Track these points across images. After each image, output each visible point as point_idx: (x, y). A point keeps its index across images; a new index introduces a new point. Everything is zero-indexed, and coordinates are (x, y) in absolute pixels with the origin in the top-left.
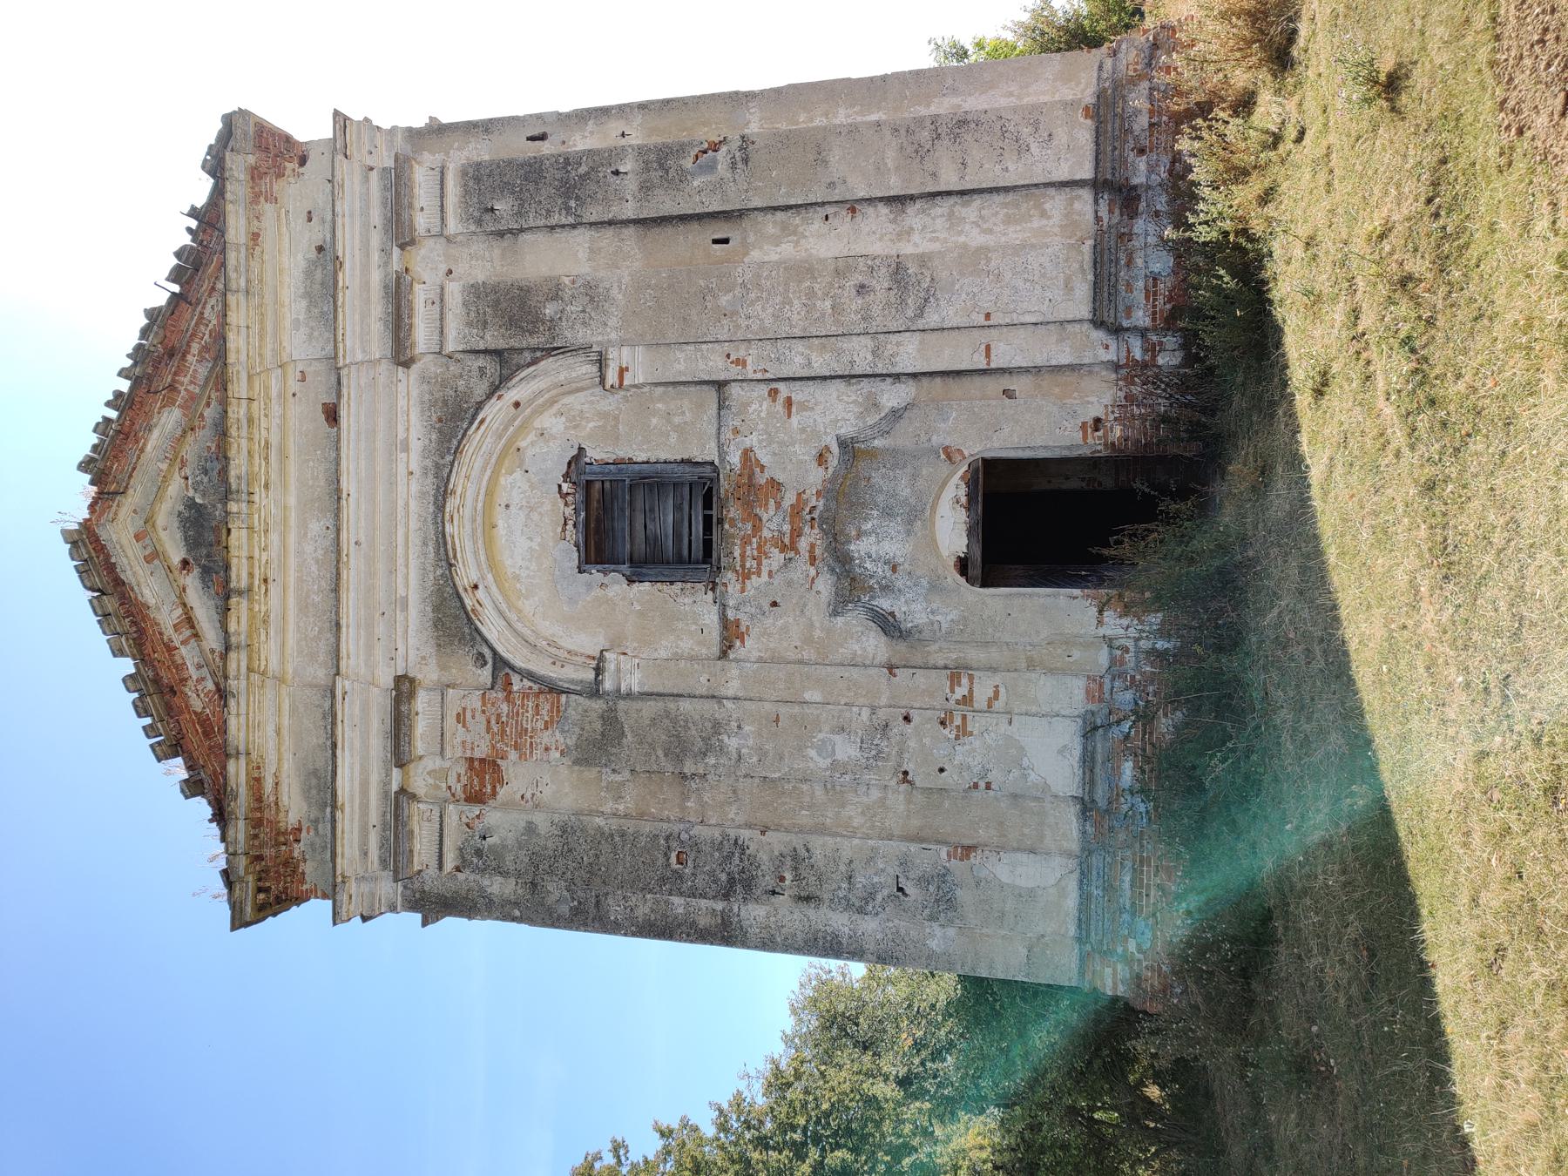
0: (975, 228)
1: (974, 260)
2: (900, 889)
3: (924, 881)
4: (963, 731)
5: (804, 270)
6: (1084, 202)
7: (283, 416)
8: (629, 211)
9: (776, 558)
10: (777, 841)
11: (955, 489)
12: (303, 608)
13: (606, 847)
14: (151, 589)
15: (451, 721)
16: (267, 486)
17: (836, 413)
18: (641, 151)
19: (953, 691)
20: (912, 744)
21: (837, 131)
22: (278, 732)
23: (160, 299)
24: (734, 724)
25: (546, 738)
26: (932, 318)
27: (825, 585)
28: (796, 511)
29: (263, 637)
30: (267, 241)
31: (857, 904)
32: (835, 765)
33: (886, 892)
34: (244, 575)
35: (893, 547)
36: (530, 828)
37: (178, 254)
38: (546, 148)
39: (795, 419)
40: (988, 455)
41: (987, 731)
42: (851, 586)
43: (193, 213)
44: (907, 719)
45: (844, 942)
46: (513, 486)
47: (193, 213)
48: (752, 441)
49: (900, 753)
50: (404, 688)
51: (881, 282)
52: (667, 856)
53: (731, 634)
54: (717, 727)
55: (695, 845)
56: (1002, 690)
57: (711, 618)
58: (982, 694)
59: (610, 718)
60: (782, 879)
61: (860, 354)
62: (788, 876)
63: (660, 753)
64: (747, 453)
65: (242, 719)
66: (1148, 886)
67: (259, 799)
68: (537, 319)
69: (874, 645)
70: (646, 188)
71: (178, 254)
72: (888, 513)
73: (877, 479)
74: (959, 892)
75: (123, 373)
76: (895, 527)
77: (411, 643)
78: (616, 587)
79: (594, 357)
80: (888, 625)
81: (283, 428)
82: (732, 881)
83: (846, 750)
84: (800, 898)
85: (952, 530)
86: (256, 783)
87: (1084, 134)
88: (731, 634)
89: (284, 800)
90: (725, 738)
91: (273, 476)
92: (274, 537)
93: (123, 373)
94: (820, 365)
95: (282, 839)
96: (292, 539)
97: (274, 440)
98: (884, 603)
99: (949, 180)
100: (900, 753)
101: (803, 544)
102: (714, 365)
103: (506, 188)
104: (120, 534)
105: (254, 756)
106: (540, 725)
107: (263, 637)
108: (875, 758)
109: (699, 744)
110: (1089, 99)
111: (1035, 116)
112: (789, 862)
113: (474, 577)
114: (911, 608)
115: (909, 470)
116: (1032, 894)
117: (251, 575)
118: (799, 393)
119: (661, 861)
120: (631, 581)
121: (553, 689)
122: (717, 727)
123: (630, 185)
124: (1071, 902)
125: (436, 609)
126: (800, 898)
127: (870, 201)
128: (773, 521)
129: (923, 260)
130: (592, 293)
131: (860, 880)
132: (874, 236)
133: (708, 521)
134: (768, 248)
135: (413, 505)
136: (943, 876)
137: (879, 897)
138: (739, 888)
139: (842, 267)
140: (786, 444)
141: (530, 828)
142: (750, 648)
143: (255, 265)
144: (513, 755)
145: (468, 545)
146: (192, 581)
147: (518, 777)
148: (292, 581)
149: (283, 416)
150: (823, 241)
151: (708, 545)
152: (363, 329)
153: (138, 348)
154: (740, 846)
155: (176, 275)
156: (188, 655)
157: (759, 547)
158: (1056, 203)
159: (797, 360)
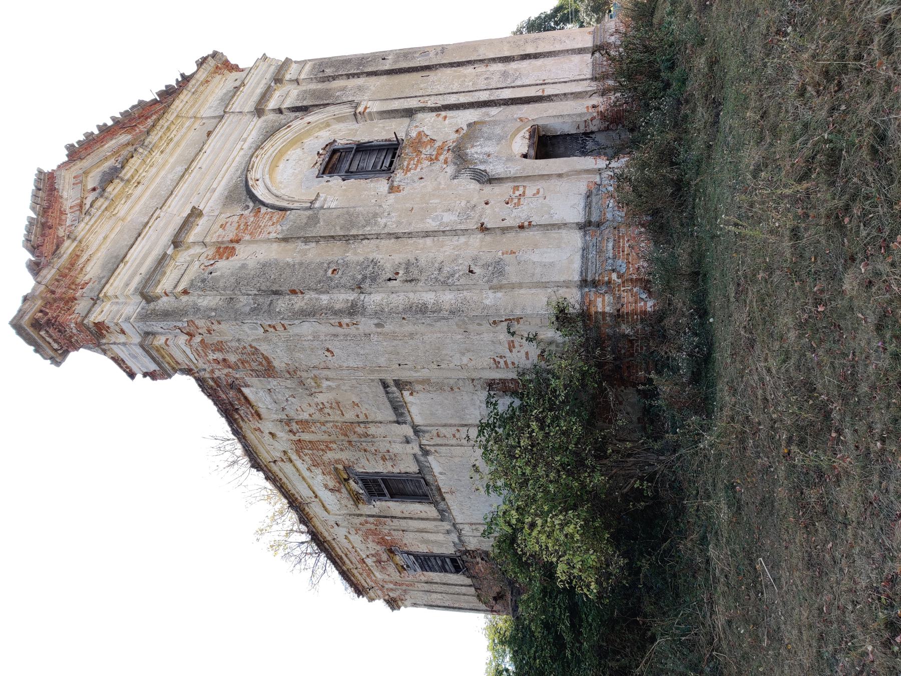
2: (471, 271)
3: (486, 266)
4: (518, 204)
6: (588, 57)
7: (186, 133)
8: (387, 68)
9: (427, 163)
10: (398, 258)
11: (525, 132)
12: (152, 197)
13: (288, 270)
15: (217, 226)
16: (162, 152)
19: (514, 193)
20: (488, 212)
22: (105, 238)
23: (149, 97)
24: (386, 214)
25: (271, 229)
26: (519, 83)
27: (450, 169)
28: (441, 148)
29: (122, 202)
30: (212, 85)
31: (442, 280)
32: (440, 225)
33: (461, 273)
34: (129, 175)
37: (166, 86)
39: (447, 121)
40: (540, 123)
43: (182, 75)
44: (487, 203)
45: (430, 307)
47: (182, 75)
48: (425, 129)
49: (481, 216)
52: (326, 271)
54: (375, 215)
55: (346, 265)
56: (541, 190)
58: (530, 192)
60: (397, 273)
61: (484, 96)
62: (401, 272)
63: (338, 228)
64: (419, 133)
65: (88, 227)
66: (623, 247)
67: (73, 265)
69: (474, 186)
70: (395, 62)
71: (166, 86)
72: (489, 139)
73: (485, 129)
74: (507, 268)
75: (113, 118)
76: (489, 143)
77: (210, 204)
78: (335, 181)
79: (354, 105)
81: (183, 137)
82: (365, 278)
83: (449, 218)
84: (407, 281)
85: (521, 144)
86: (75, 257)
88: (392, 189)
89: (88, 268)
90: (379, 219)
91: (168, 150)
92: (154, 170)
93: (113, 118)
94: (463, 99)
95: (73, 287)
96: (162, 173)
97: (175, 140)
98: (482, 167)
99: (530, 50)
100: (481, 216)
101: (442, 158)
102: (413, 104)
105: (83, 244)
106: (271, 223)
107: (122, 202)
108: (466, 219)
109: (363, 222)
112: (403, 266)
113: (258, 177)
114: (495, 168)
115: (501, 125)
116: (552, 264)
117: (132, 177)
118: (450, 113)
119: (322, 272)
120: (344, 180)
122: (375, 215)
124: (577, 264)
125: (230, 192)
126: (407, 281)
127: (494, 60)
128: (427, 151)
129: (516, 70)
131: (446, 269)
135: (238, 159)
136: (498, 263)
137: (457, 275)
138: (368, 280)
143: (202, 88)
144: (247, 237)
145: (261, 167)
148: (152, 187)
149: (186, 133)
153: (127, 111)
154: (374, 262)
155: (160, 94)
157: (418, 161)
158: (576, 58)
159: (452, 100)
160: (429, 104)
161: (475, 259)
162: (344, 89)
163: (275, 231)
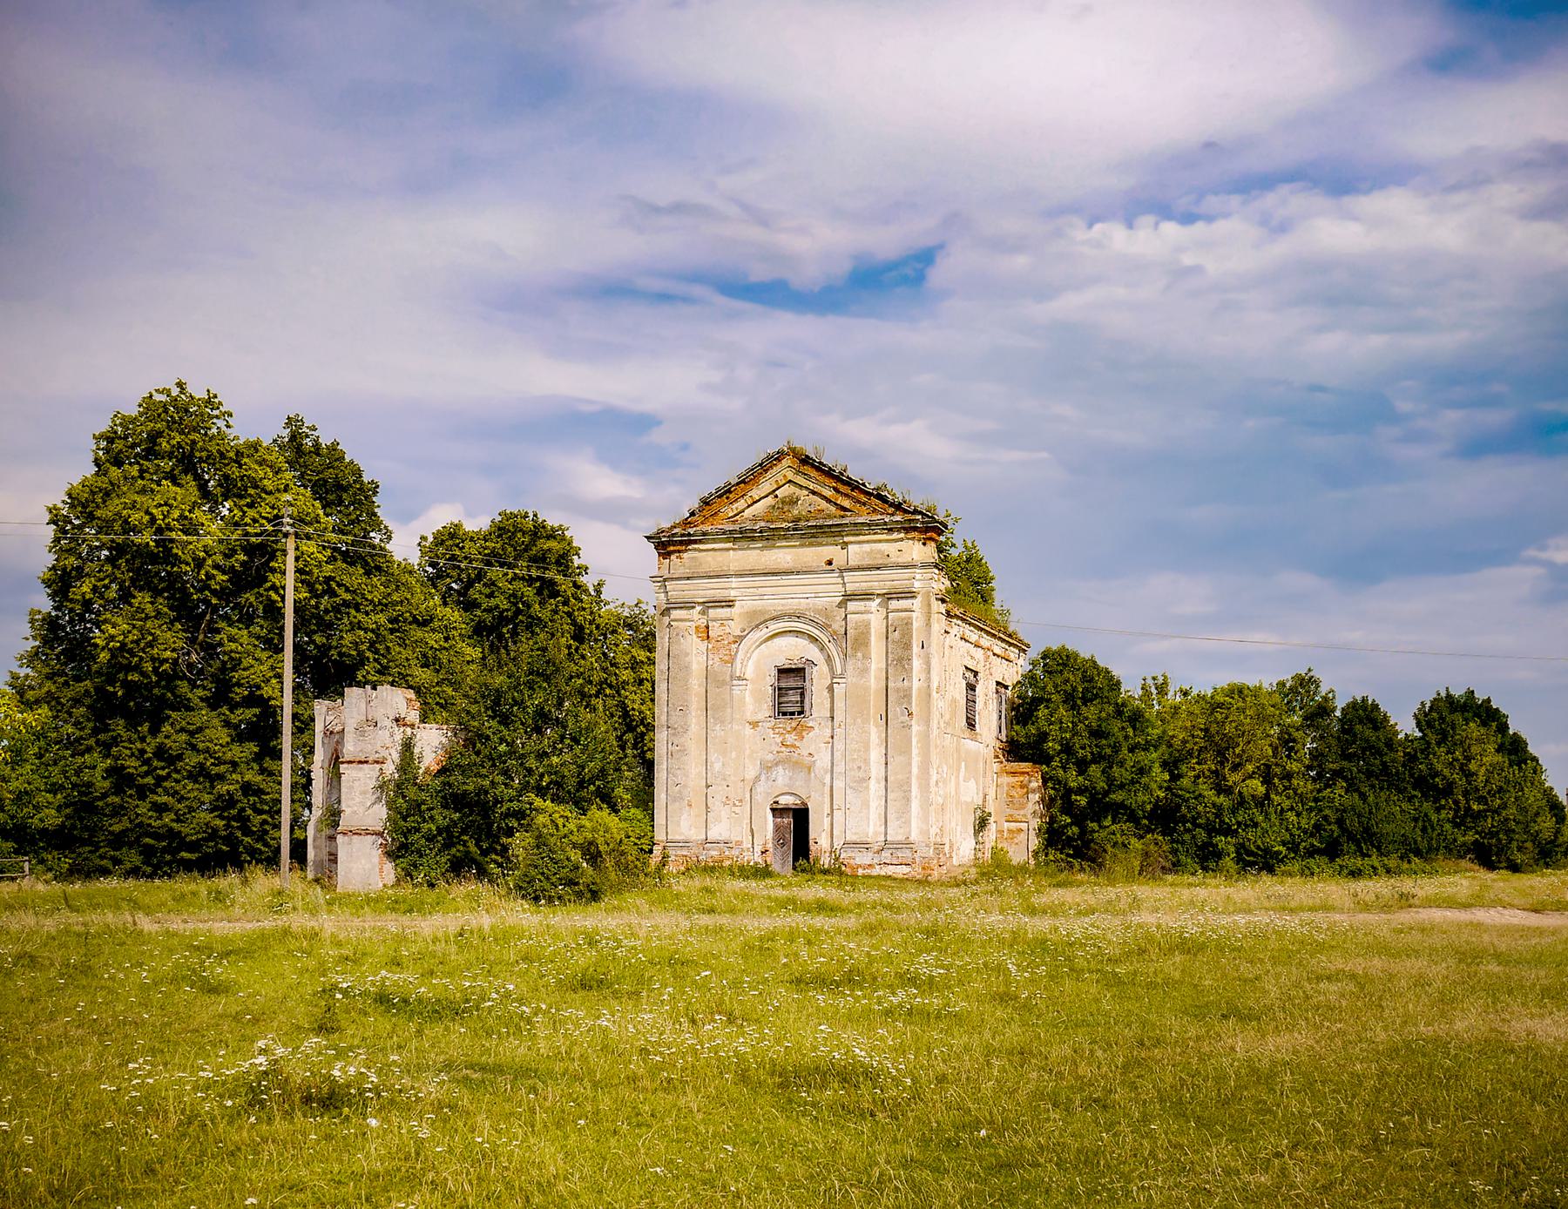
0: (876, 805)
1: (866, 804)
5: (867, 748)
9: (779, 740)
14: (766, 486)
17: (823, 760)
18: (911, 688)
21: (910, 758)
23: (870, 487)
35: (780, 781)
36: (687, 654)
38: (916, 649)
41: (724, 812)
42: (767, 767)
46: (803, 642)
50: (729, 604)
51: (861, 774)
53: (754, 724)
55: (685, 716)
57: (760, 717)
58: (737, 809)
59: (724, 683)
61: (839, 769)
68: (855, 650)
69: (751, 773)
70: (898, 690)
76: (787, 781)
80: (757, 779)
83: (717, 766)
85: (786, 801)
86: (695, 542)
87: (900, 838)
88: (754, 724)
94: (837, 755)
98: (763, 778)
103: (903, 636)
104: (784, 470)
110: (912, 839)
111: (908, 822)
114: (761, 788)
121: (732, 661)
122: (722, 722)
123: (900, 684)
124: (678, 838)
129: (867, 788)
130: (864, 671)
132: (876, 770)
133: (792, 714)
134: (875, 734)
139: (867, 761)
140: (815, 741)
141: (687, 654)
142: (748, 730)
146: (770, 500)
147: (703, 646)
150: (876, 755)
151: (785, 714)
152: (855, 582)
156: (741, 504)
160: (837, 731)
161: (685, 786)
162: (867, 657)
163: (715, 662)
